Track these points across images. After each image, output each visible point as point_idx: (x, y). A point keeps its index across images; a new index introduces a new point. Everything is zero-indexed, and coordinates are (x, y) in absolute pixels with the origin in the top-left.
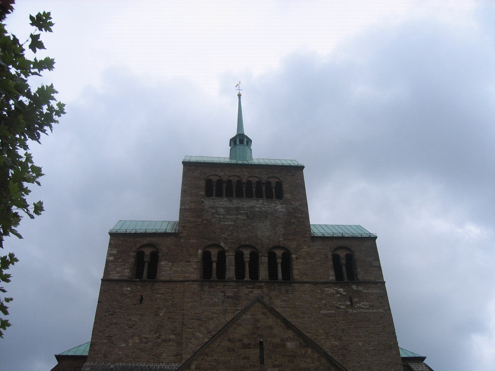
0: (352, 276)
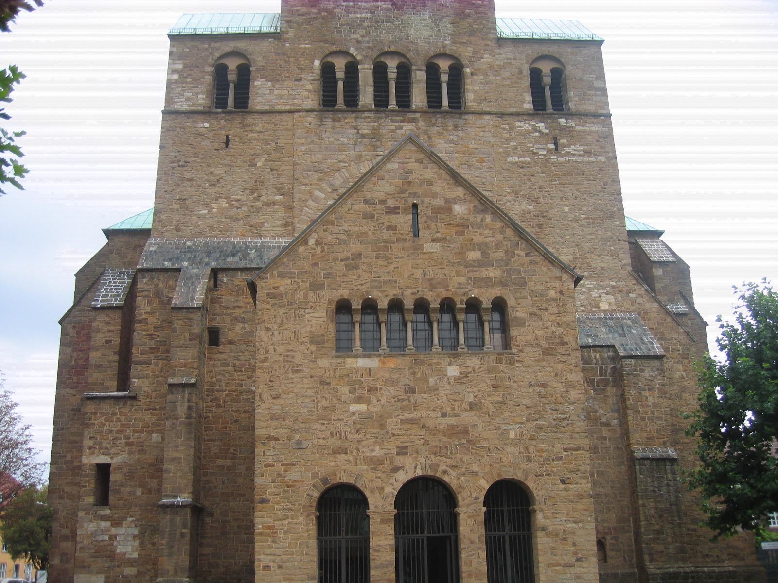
0: (559, 104)
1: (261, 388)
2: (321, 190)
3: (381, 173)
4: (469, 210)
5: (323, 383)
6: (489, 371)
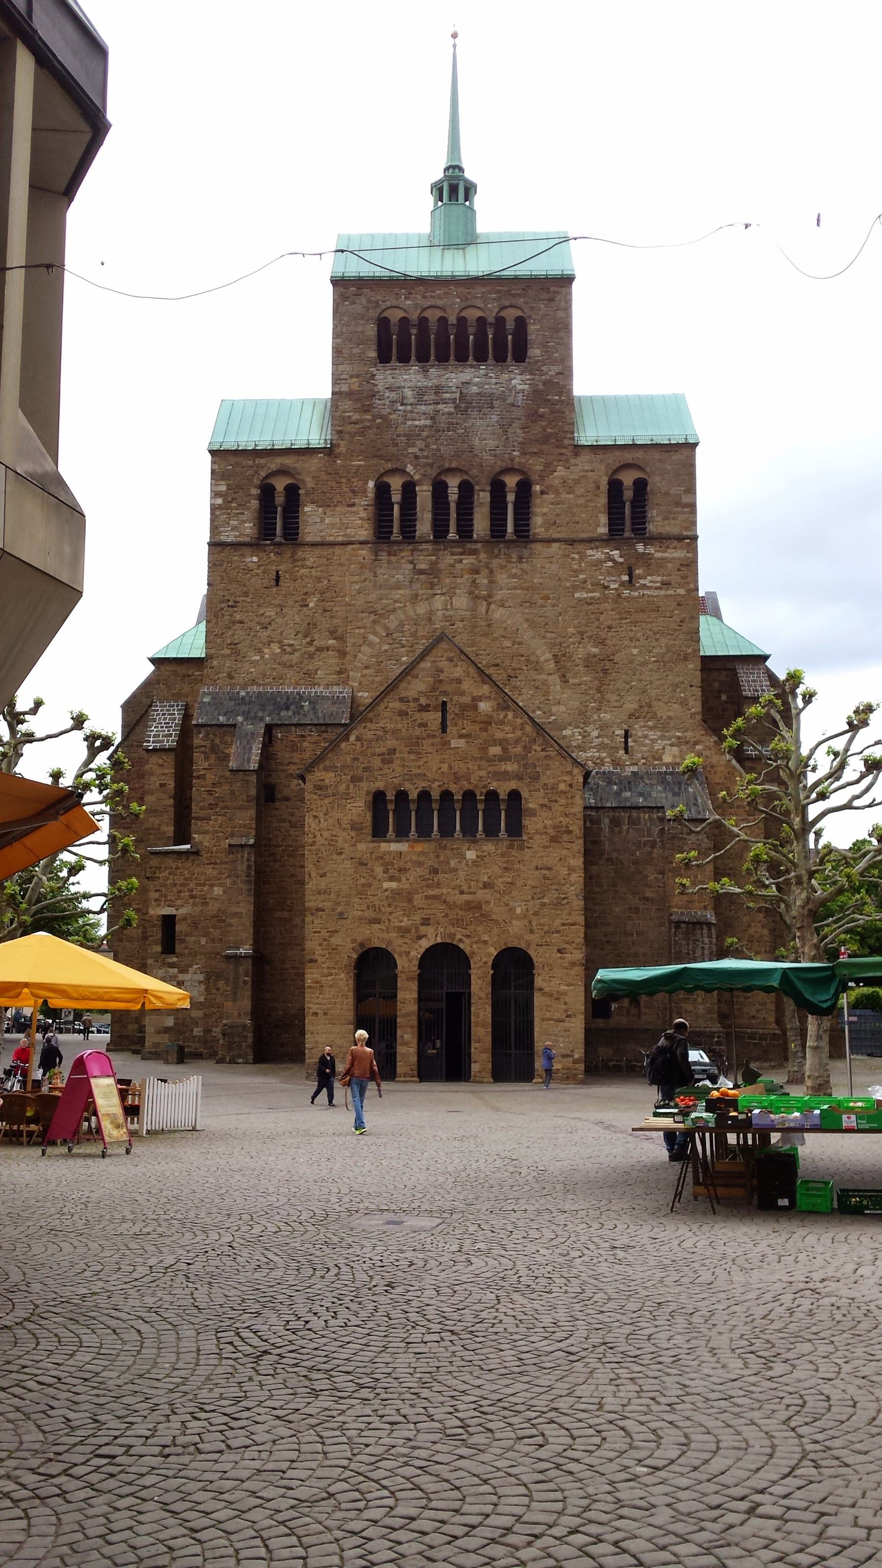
1: (310, 866)
2: (375, 633)
3: (415, 672)
4: (493, 707)
5: (362, 864)
6: (503, 856)
